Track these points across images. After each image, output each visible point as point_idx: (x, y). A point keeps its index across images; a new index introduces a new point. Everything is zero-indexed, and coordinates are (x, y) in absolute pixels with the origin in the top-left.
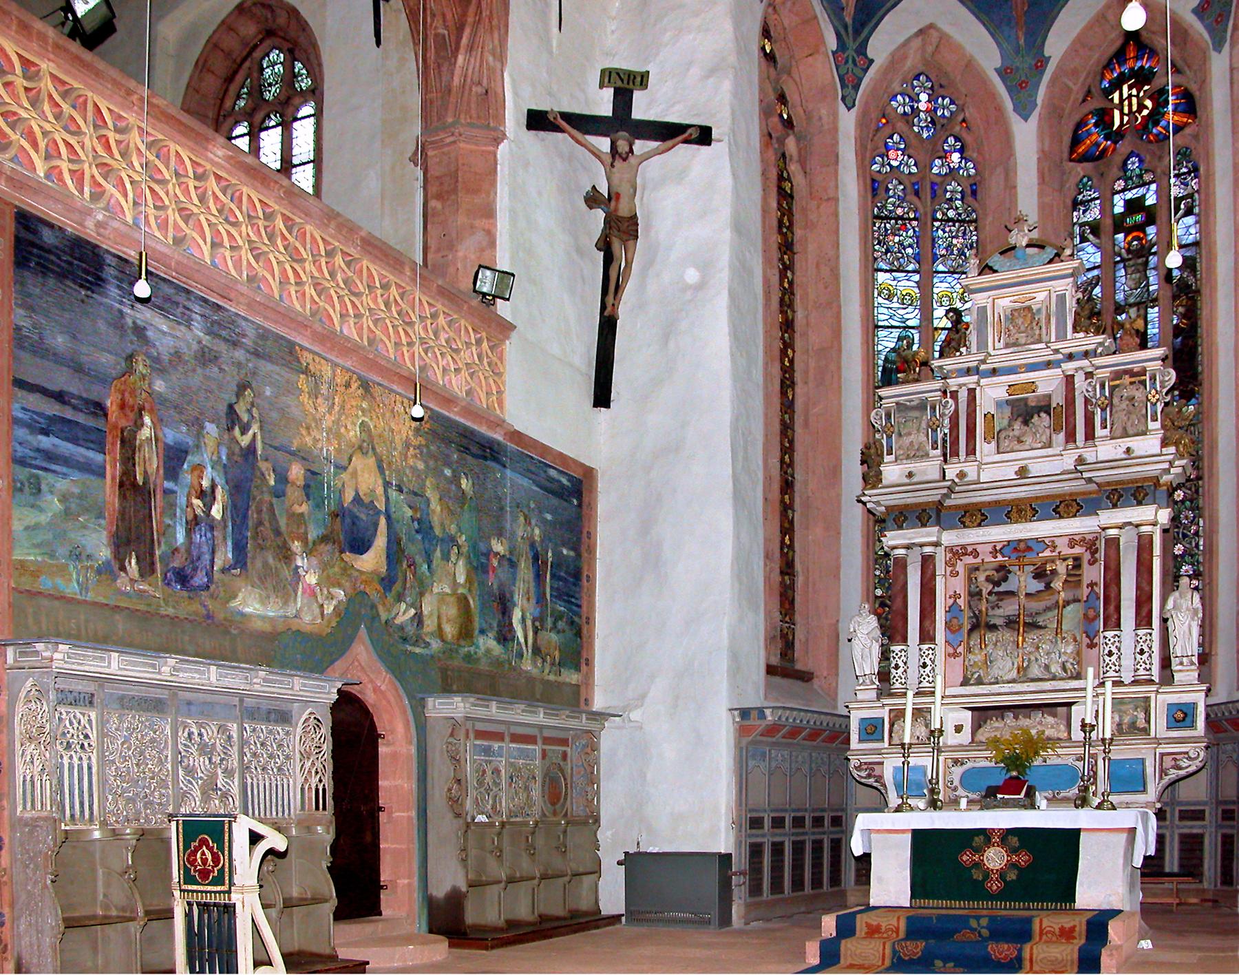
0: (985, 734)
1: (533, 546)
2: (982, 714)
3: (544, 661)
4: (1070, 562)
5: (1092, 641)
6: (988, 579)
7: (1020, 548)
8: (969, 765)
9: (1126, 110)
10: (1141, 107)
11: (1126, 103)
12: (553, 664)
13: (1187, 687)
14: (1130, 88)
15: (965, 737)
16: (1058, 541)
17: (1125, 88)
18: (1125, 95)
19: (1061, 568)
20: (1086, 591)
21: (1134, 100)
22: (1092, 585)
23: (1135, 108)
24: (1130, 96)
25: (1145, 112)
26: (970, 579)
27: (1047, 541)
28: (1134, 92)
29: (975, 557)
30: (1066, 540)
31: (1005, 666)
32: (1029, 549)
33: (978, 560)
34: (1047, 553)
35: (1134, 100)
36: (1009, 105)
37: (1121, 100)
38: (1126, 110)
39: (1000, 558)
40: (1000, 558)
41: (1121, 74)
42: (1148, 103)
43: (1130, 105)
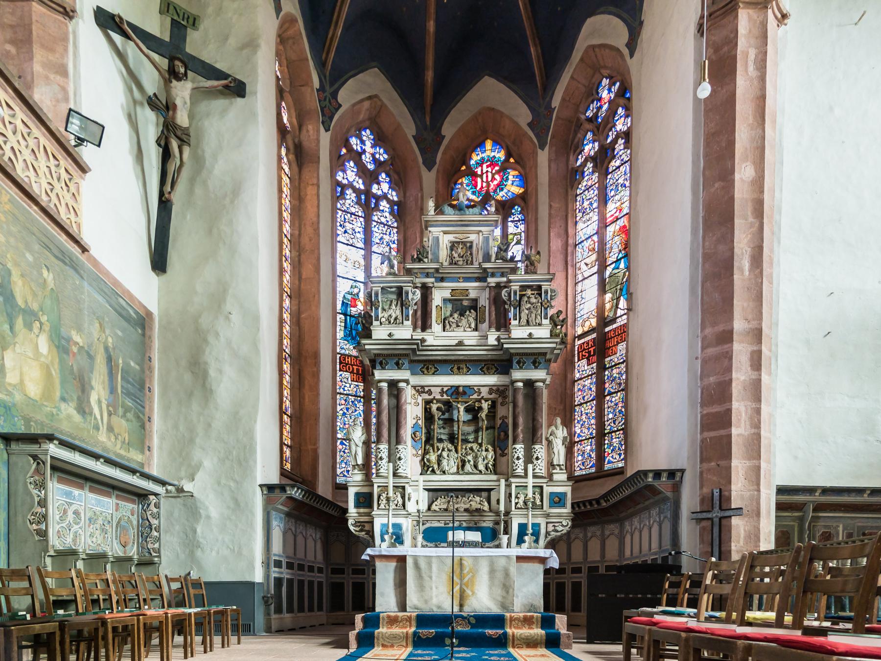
0: (438, 505)
1: (106, 349)
2: (435, 492)
3: (116, 438)
4: (490, 402)
5: (503, 452)
6: (438, 409)
7: (456, 391)
8: (428, 525)
9: (485, 179)
10: (493, 179)
11: (485, 176)
12: (123, 442)
13: (560, 484)
14: (487, 167)
15: (423, 506)
16: (482, 389)
17: (485, 166)
18: (484, 171)
19: (485, 405)
20: (499, 422)
21: (490, 175)
22: (504, 418)
23: (490, 179)
24: (487, 172)
25: (495, 182)
26: (426, 409)
27: (476, 388)
28: (489, 169)
29: (430, 395)
30: (487, 389)
31: (450, 463)
32: (464, 393)
33: (431, 397)
34: (475, 396)
35: (490, 175)
36: (420, 160)
37: (482, 173)
38: (485, 179)
39: (445, 397)
40: (445, 397)
41: (483, 159)
42: (497, 177)
43: (487, 176)
